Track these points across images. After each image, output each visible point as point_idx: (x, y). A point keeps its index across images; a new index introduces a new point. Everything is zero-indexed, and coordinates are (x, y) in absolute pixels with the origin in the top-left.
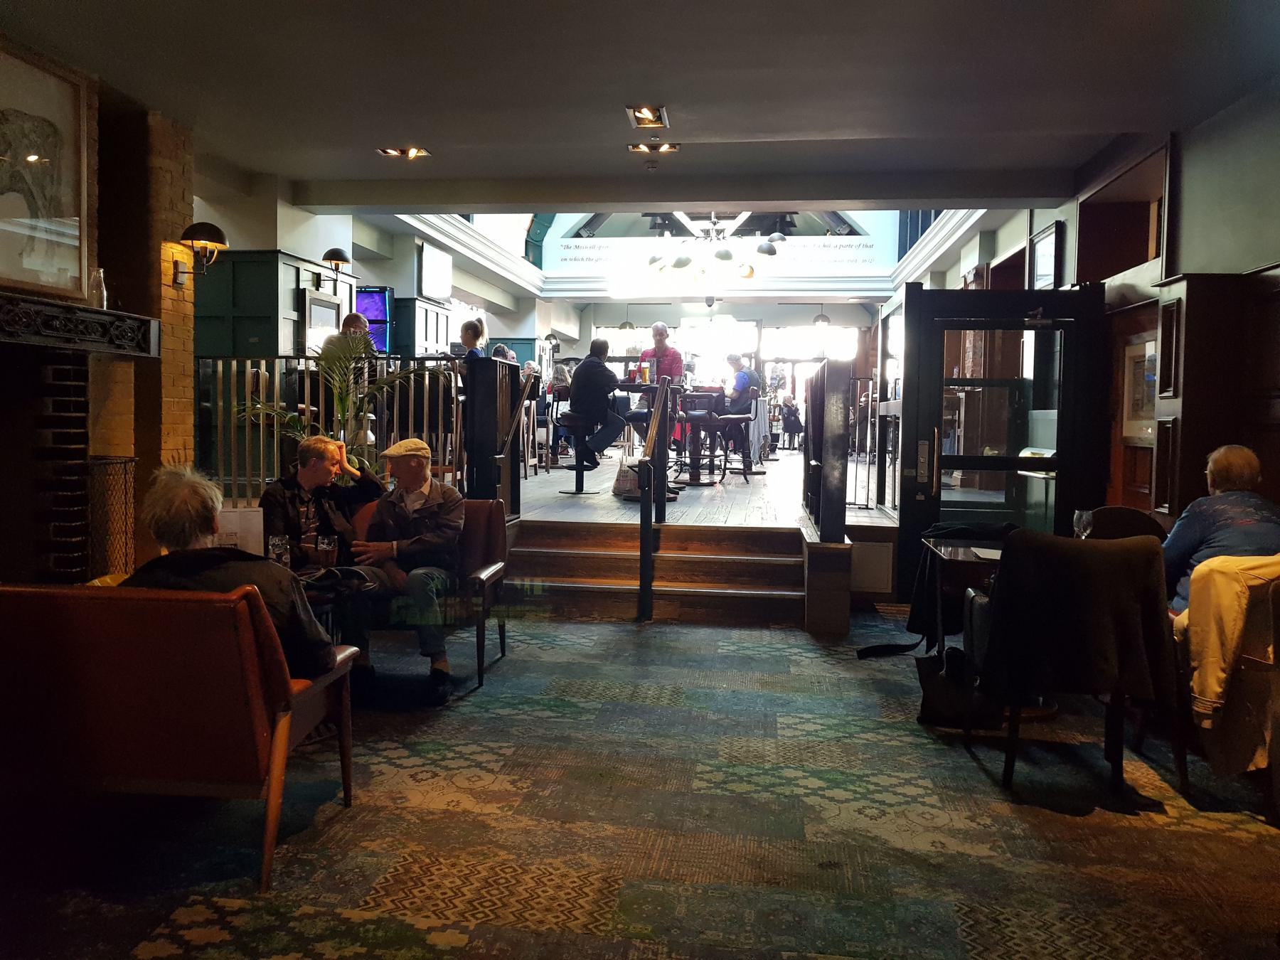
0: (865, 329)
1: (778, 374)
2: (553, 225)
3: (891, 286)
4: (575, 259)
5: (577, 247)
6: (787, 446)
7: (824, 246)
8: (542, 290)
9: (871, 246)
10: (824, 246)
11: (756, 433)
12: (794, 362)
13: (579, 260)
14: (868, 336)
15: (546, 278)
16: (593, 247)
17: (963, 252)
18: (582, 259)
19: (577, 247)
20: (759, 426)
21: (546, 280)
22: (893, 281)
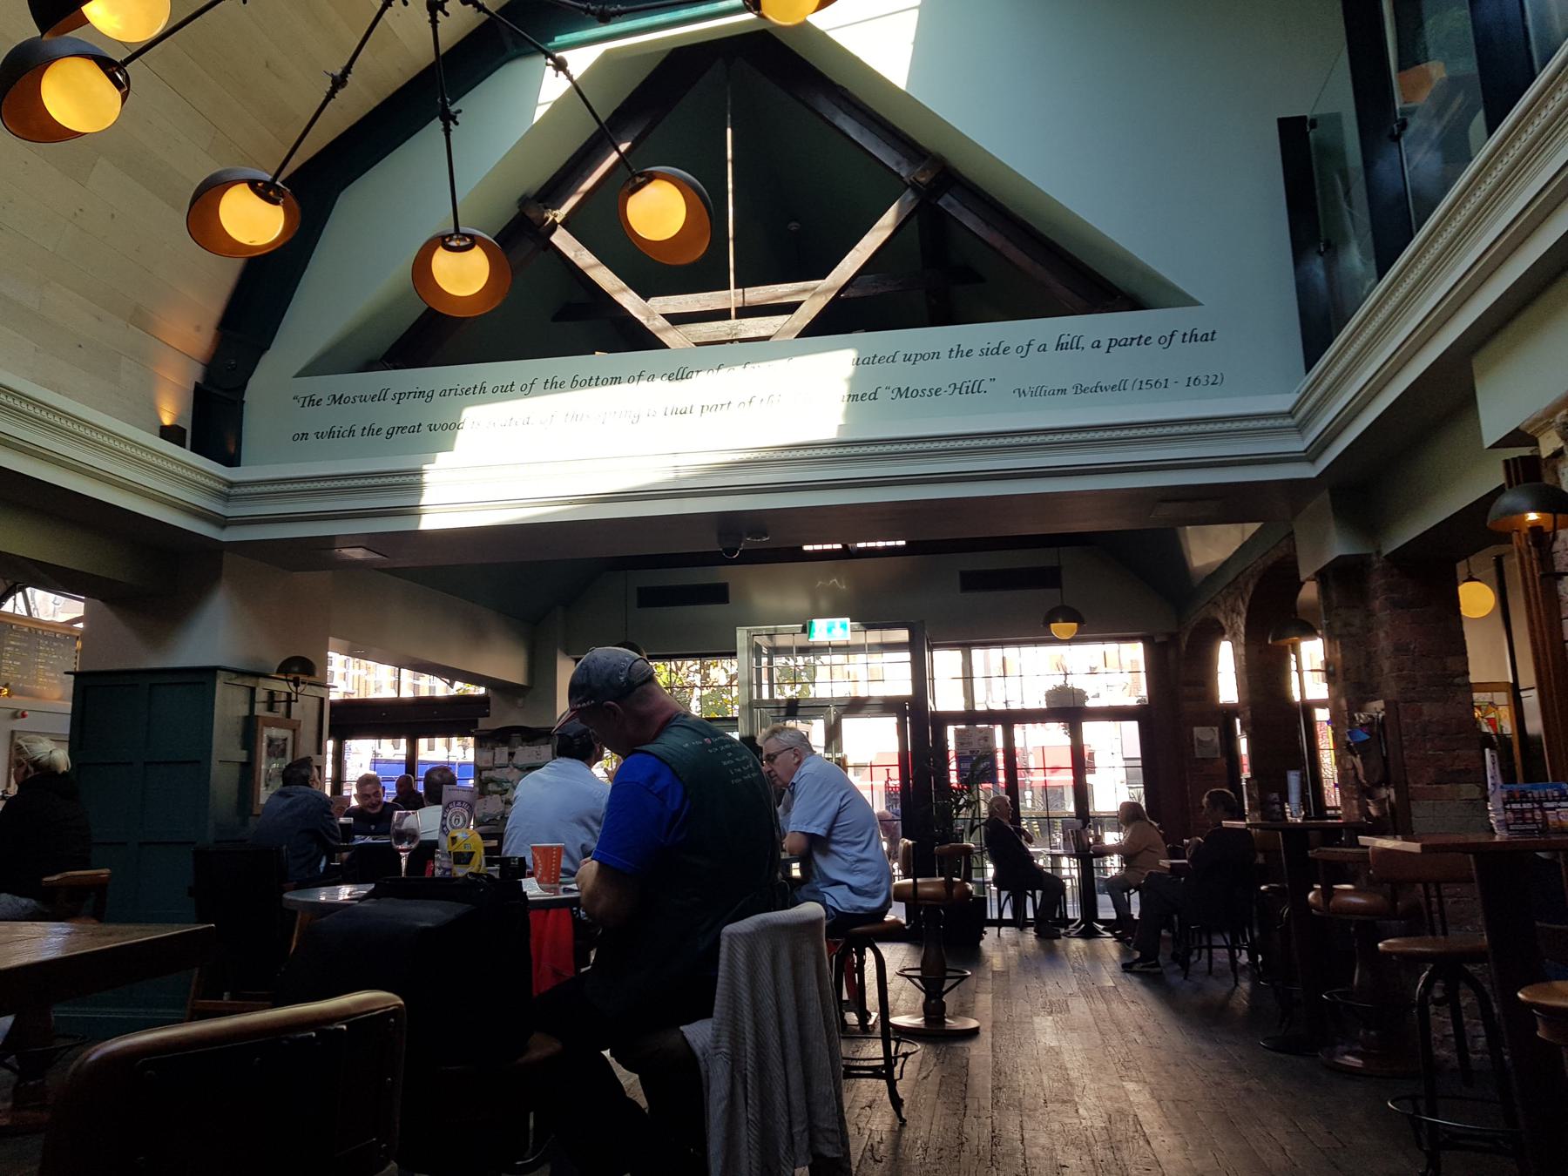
0: (1164, 639)
1: (975, 746)
2: (273, 346)
3: (1299, 445)
4: (331, 434)
5: (336, 400)
6: (1008, 915)
7: (1060, 346)
8: (223, 522)
9: (1208, 337)
10: (1060, 346)
11: (747, 1137)
12: (1009, 719)
13: (340, 434)
14: (1172, 654)
15: (231, 484)
16: (381, 397)
17: (1477, 363)
18: (352, 432)
19: (336, 400)
20: (765, 1105)
21: (229, 492)
22: (1301, 428)
